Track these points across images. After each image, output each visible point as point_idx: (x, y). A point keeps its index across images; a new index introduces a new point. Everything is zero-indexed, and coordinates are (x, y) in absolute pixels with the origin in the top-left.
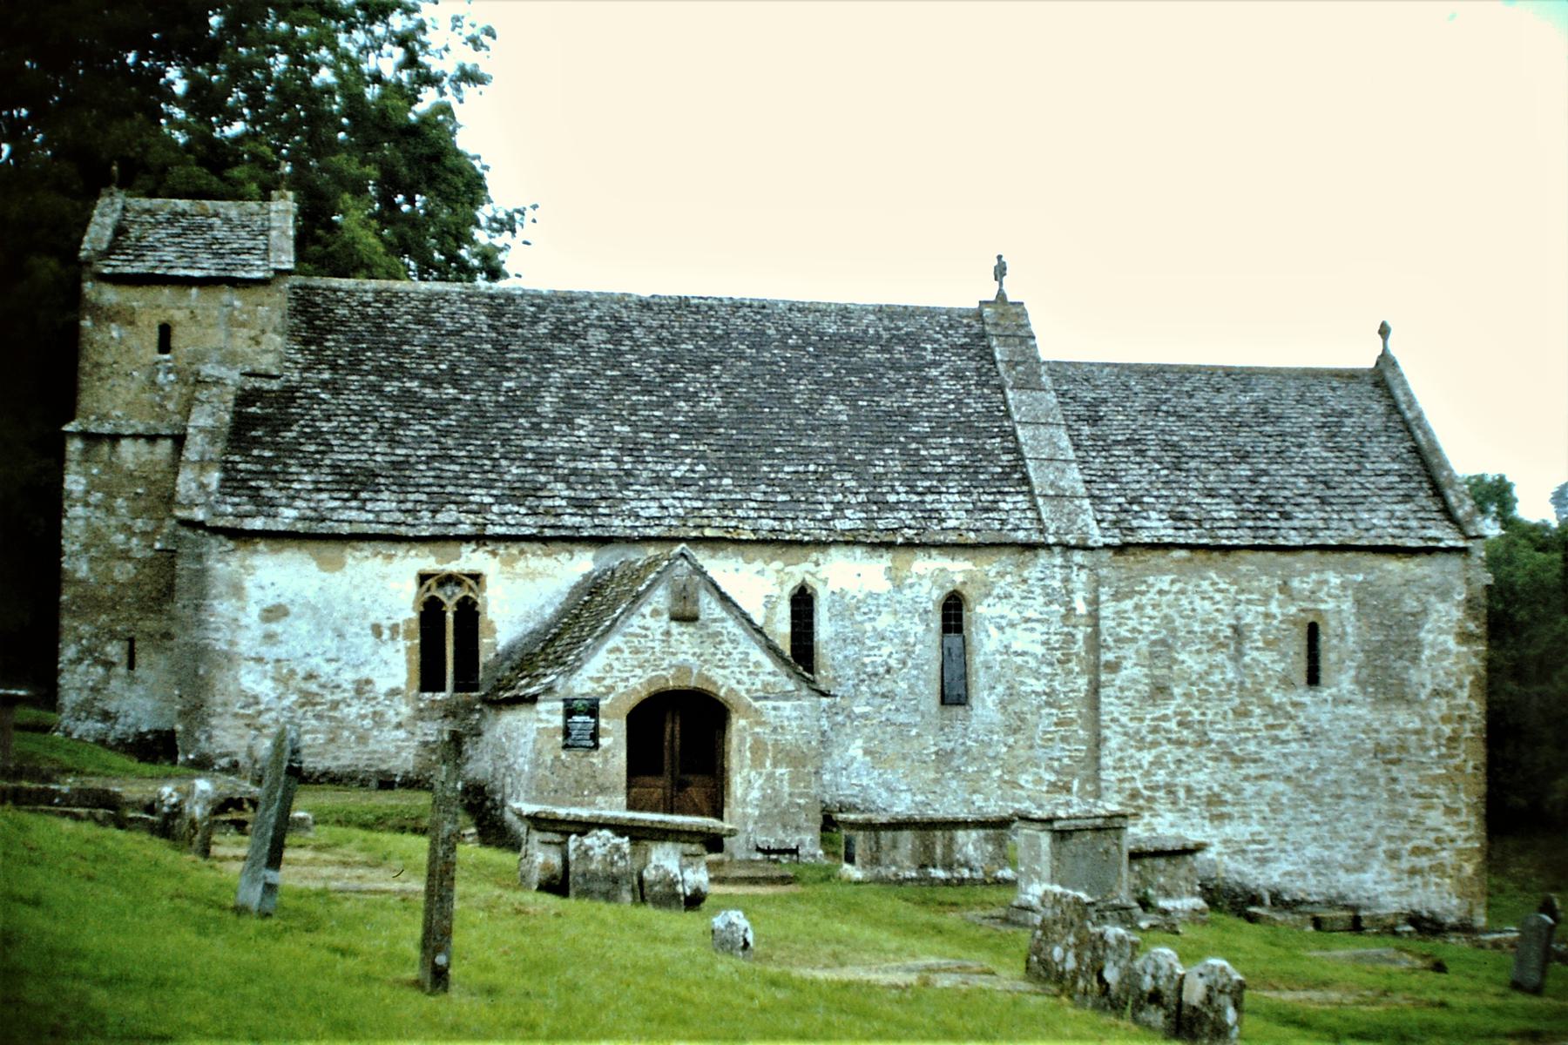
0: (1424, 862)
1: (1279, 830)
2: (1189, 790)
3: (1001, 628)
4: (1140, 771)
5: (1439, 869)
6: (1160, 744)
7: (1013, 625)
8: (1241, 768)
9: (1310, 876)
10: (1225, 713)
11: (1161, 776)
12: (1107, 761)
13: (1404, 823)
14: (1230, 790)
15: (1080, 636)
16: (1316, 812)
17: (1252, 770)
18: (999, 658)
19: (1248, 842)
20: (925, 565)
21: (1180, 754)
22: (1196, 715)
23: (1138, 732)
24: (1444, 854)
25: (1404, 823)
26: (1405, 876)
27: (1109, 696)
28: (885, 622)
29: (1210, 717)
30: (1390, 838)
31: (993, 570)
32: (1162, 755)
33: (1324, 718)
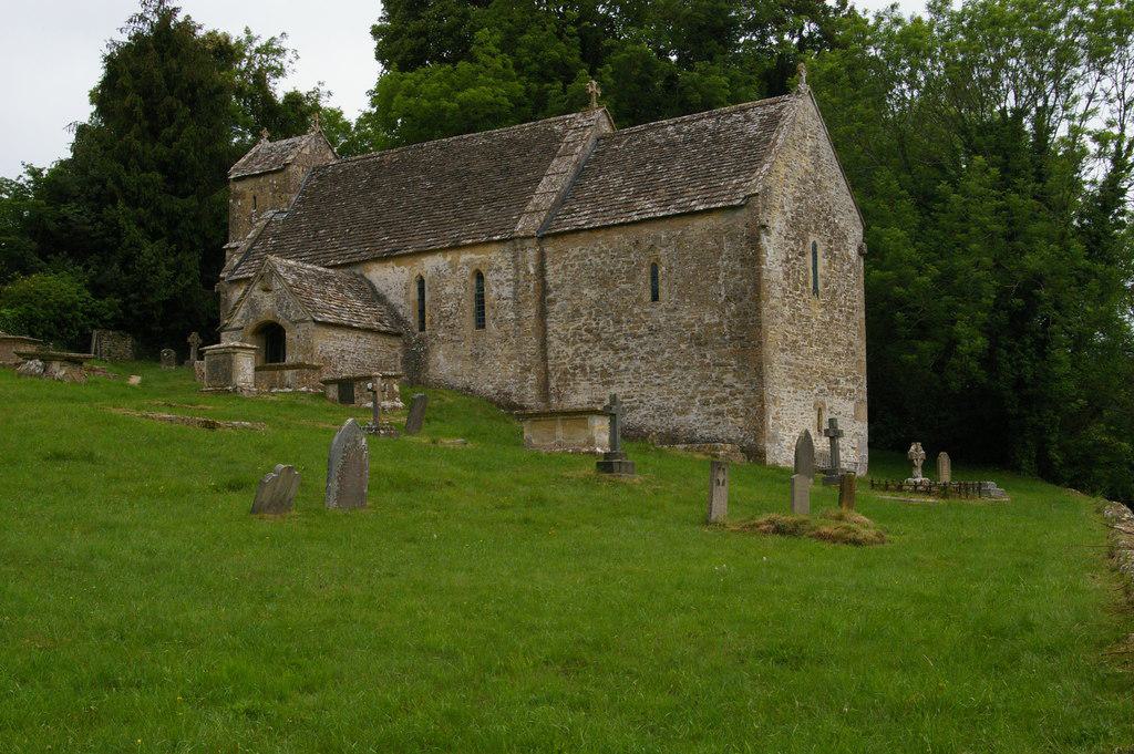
0: (724, 407)
2: (592, 367)
3: (497, 286)
5: (735, 412)
6: (577, 343)
7: (502, 284)
11: (578, 361)
13: (710, 383)
15: (532, 286)
20: (465, 256)
21: (586, 348)
23: (566, 336)
24: (737, 402)
25: (710, 383)
28: (449, 290)
30: (703, 393)
31: (493, 255)
32: (578, 349)
33: (662, 320)
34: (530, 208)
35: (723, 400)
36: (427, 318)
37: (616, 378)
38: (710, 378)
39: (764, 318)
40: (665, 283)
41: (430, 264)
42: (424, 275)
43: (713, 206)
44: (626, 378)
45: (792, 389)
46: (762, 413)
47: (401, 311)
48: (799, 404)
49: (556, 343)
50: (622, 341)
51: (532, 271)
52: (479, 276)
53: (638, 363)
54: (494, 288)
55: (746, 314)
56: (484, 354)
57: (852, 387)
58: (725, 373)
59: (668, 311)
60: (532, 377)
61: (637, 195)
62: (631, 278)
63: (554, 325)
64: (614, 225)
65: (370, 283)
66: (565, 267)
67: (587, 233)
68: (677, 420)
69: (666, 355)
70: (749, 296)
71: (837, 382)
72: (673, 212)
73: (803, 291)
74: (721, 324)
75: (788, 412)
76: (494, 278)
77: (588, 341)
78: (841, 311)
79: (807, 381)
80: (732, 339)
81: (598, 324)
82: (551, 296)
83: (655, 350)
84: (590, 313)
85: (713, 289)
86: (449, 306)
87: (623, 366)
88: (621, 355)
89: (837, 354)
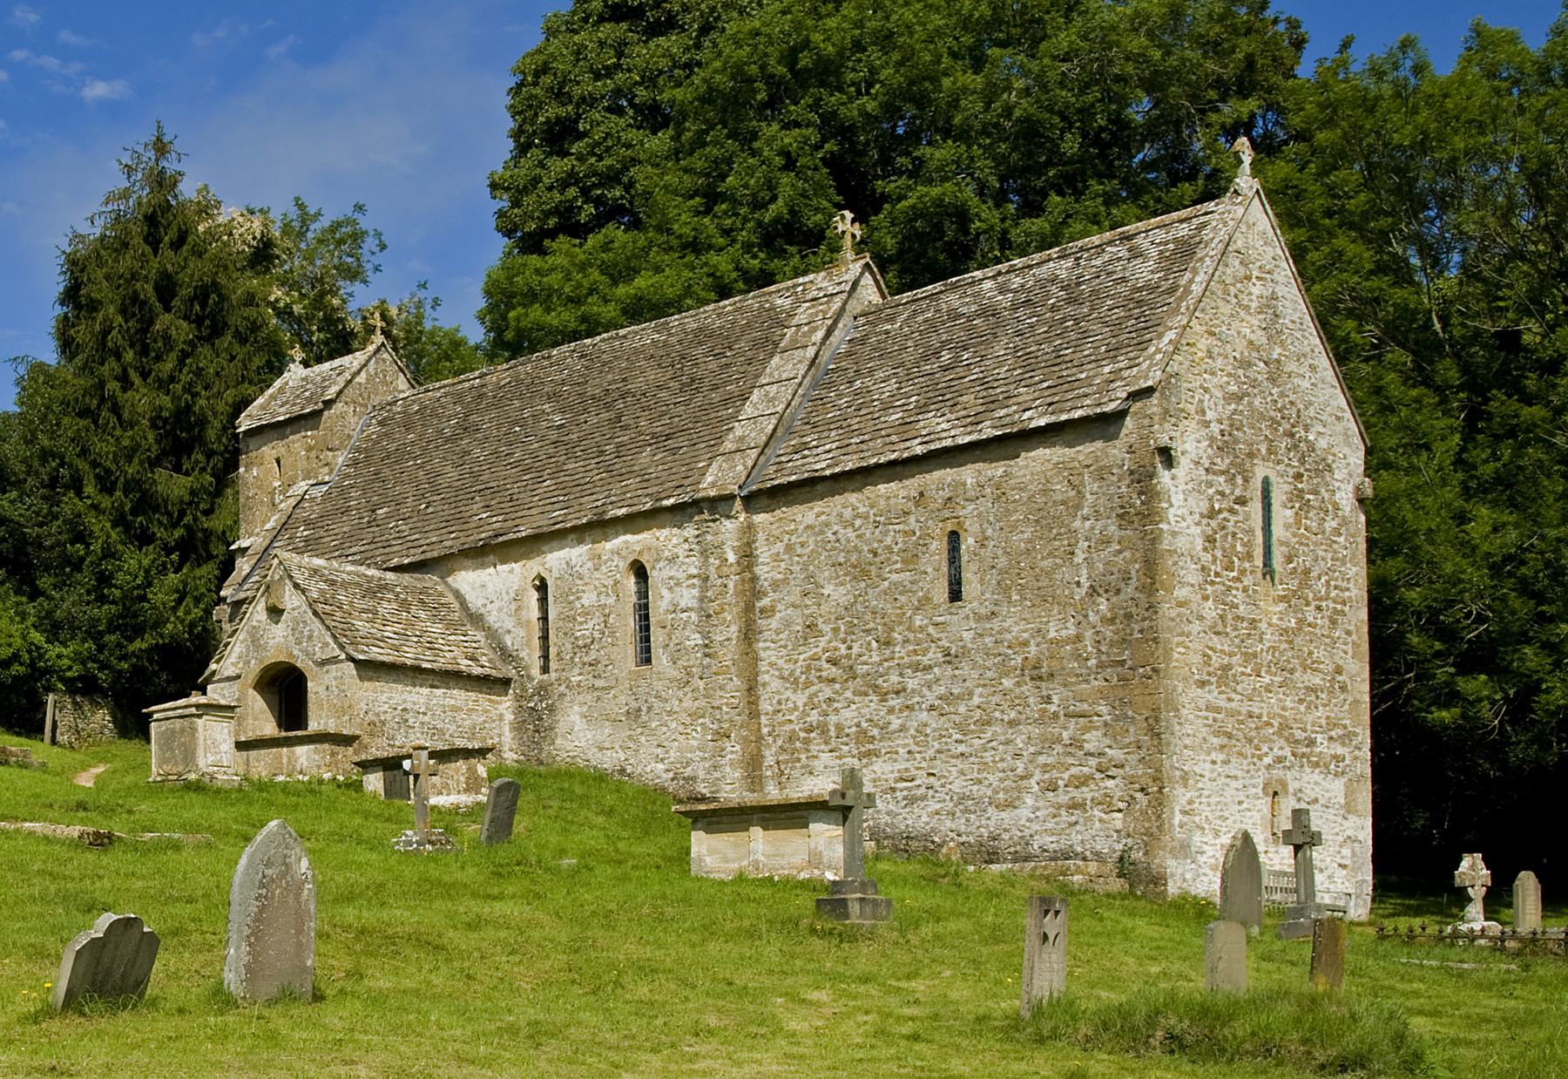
0: (1086, 793)
1: (924, 764)
2: (839, 727)
4: (796, 713)
5: (1106, 803)
8: (886, 701)
9: (958, 814)
10: (869, 644)
11: (814, 717)
12: (765, 706)
14: (876, 726)
16: (962, 742)
17: (895, 702)
18: (670, 617)
19: (896, 781)
22: (843, 650)
23: (792, 673)
26: (1063, 813)
27: (765, 641)
28: (588, 599)
29: (856, 650)
30: (1046, 768)
34: (729, 445)
35: (1083, 781)
36: (553, 651)
37: (883, 746)
38: (1059, 740)
39: (1163, 623)
40: (973, 567)
41: (556, 561)
42: (545, 575)
43: (1064, 417)
44: (902, 743)
45: (1221, 757)
46: (1159, 802)
47: (508, 640)
48: (1234, 784)
49: (776, 684)
50: (895, 678)
51: (732, 558)
52: (640, 571)
53: (924, 716)
54: (665, 592)
55: (1129, 616)
56: (649, 709)
57: (1340, 751)
58: (1087, 729)
59: (979, 618)
60: (733, 749)
61: (922, 409)
62: (910, 559)
63: (768, 651)
64: (878, 466)
65: (458, 595)
66: (789, 548)
67: (828, 484)
68: (995, 819)
69: (976, 700)
70: (1134, 582)
71: (1311, 743)
72: (988, 432)
73: (1243, 572)
74: (1079, 638)
75: (1213, 800)
76: (667, 573)
77: (833, 680)
78: (1319, 608)
79: (1250, 741)
80: (1101, 665)
81: (850, 648)
82: (765, 602)
83: (955, 691)
84: (836, 630)
85: (1065, 573)
86: (588, 628)
87: (896, 723)
88: (891, 703)
89: (1311, 690)
